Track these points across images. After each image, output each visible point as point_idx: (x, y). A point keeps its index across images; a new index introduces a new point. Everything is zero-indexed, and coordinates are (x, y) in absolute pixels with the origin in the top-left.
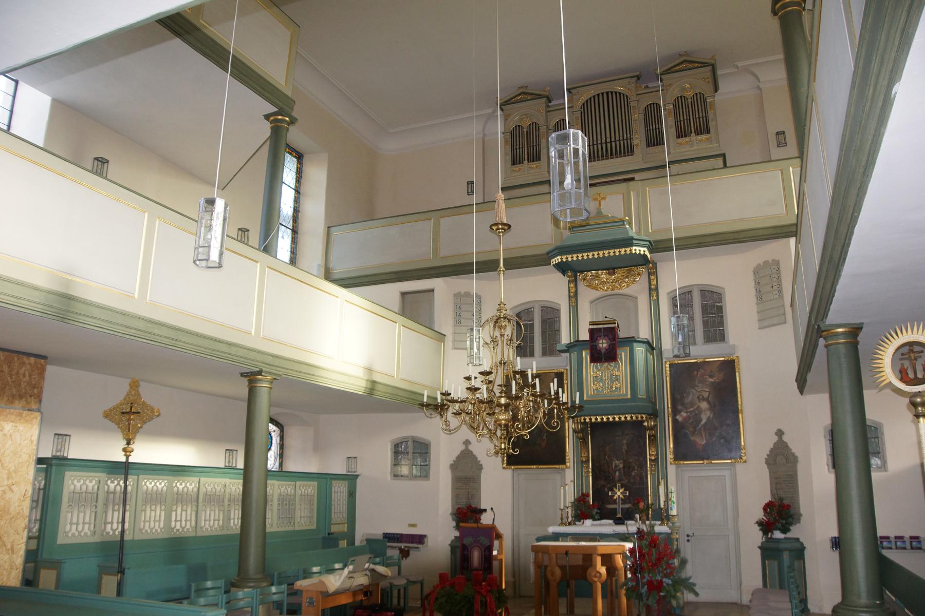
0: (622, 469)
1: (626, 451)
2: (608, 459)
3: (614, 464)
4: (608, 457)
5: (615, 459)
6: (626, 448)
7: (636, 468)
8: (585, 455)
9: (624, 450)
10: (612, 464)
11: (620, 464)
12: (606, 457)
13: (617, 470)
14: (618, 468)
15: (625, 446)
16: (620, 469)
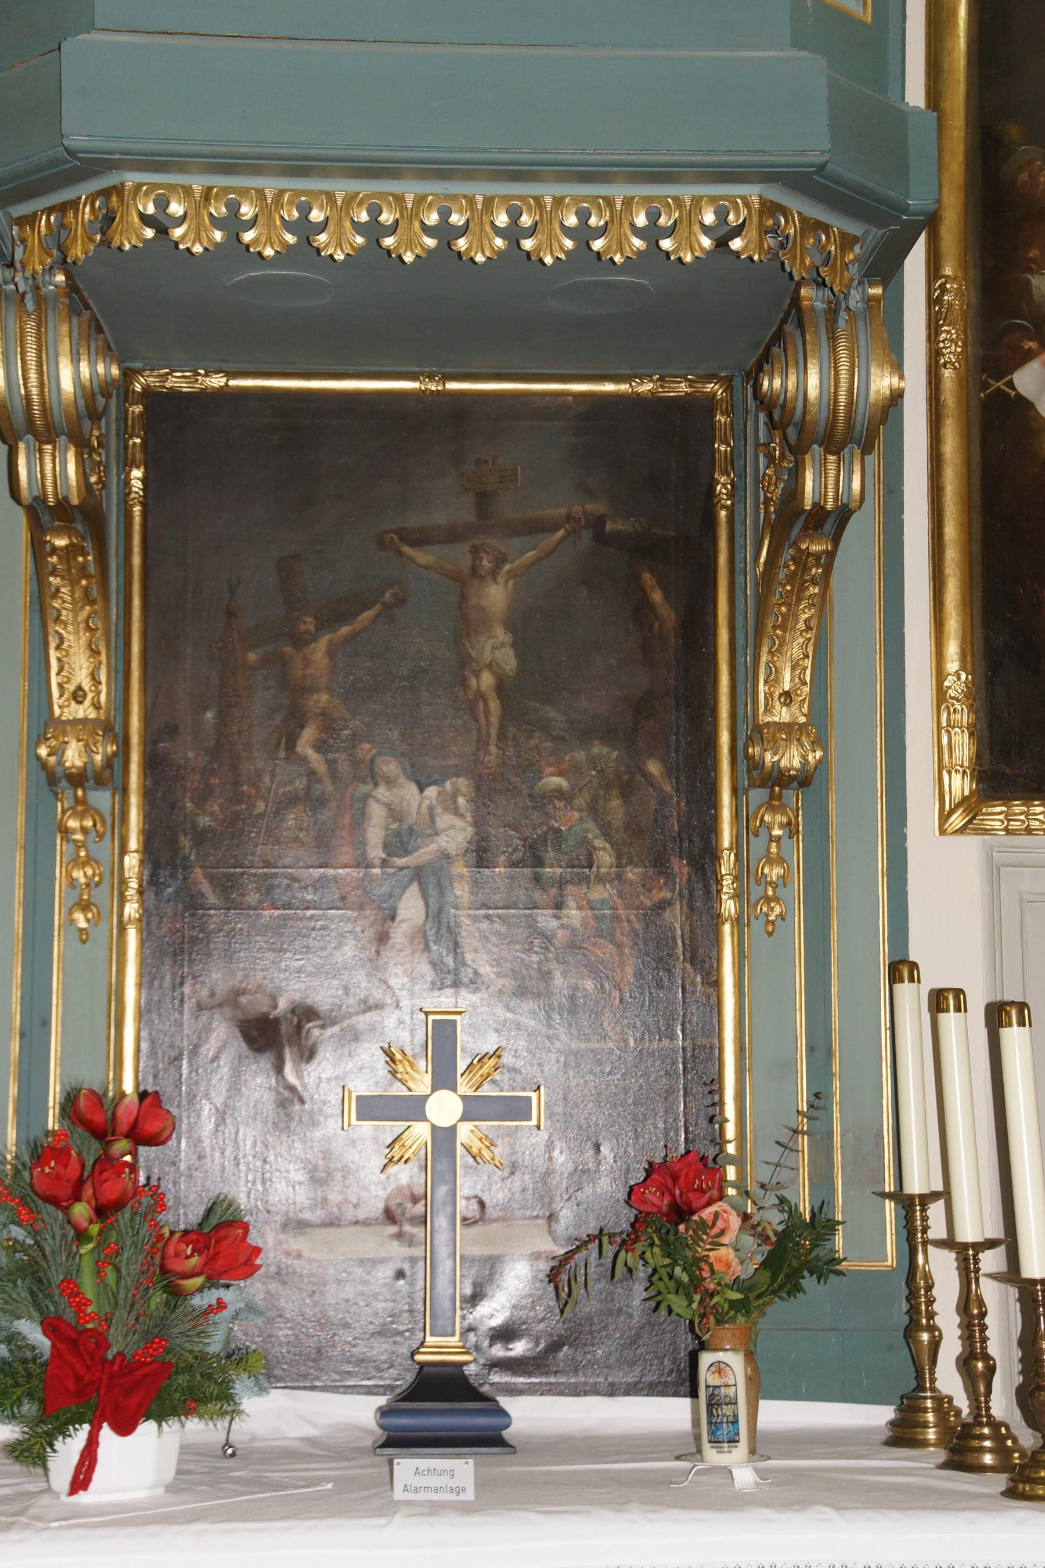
0: (460, 869)
1: (500, 688)
2: (316, 759)
3: (377, 813)
4: (320, 747)
5: (390, 767)
6: (508, 660)
7: (605, 857)
8: (83, 711)
9: (487, 679)
10: (360, 819)
11: (444, 820)
12: (305, 746)
13: (418, 874)
14: (424, 853)
15: (501, 634)
16: (446, 856)
